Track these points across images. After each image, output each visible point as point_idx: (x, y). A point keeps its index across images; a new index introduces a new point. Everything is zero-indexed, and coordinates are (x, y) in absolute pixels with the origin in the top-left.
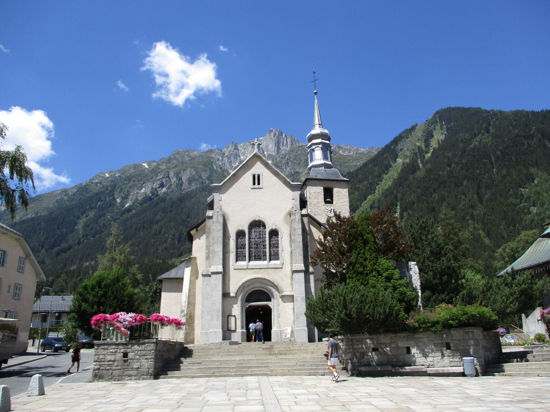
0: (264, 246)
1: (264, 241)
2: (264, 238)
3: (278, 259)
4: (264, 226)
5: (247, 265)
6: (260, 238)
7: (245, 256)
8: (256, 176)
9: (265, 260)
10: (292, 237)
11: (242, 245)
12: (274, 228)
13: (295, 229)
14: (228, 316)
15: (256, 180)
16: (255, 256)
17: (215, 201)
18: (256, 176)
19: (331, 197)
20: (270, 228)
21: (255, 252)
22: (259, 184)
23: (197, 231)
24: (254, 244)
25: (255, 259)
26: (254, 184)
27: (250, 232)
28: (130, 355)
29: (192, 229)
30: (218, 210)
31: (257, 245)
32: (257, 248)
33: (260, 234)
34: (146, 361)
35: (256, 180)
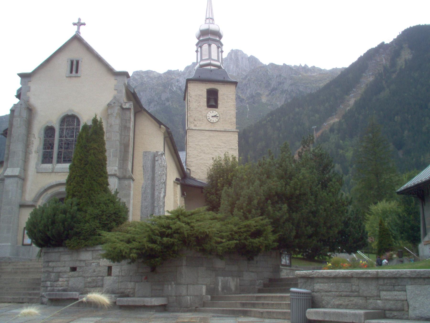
5: (53, 168)
6: (72, 136)
8: (75, 63)
11: (50, 144)
16: (64, 158)
18: (75, 63)
21: (65, 153)
22: (77, 72)
24: (65, 144)
25: (64, 161)
26: (71, 72)
27: (62, 130)
31: (68, 144)
32: (67, 148)
33: (73, 132)
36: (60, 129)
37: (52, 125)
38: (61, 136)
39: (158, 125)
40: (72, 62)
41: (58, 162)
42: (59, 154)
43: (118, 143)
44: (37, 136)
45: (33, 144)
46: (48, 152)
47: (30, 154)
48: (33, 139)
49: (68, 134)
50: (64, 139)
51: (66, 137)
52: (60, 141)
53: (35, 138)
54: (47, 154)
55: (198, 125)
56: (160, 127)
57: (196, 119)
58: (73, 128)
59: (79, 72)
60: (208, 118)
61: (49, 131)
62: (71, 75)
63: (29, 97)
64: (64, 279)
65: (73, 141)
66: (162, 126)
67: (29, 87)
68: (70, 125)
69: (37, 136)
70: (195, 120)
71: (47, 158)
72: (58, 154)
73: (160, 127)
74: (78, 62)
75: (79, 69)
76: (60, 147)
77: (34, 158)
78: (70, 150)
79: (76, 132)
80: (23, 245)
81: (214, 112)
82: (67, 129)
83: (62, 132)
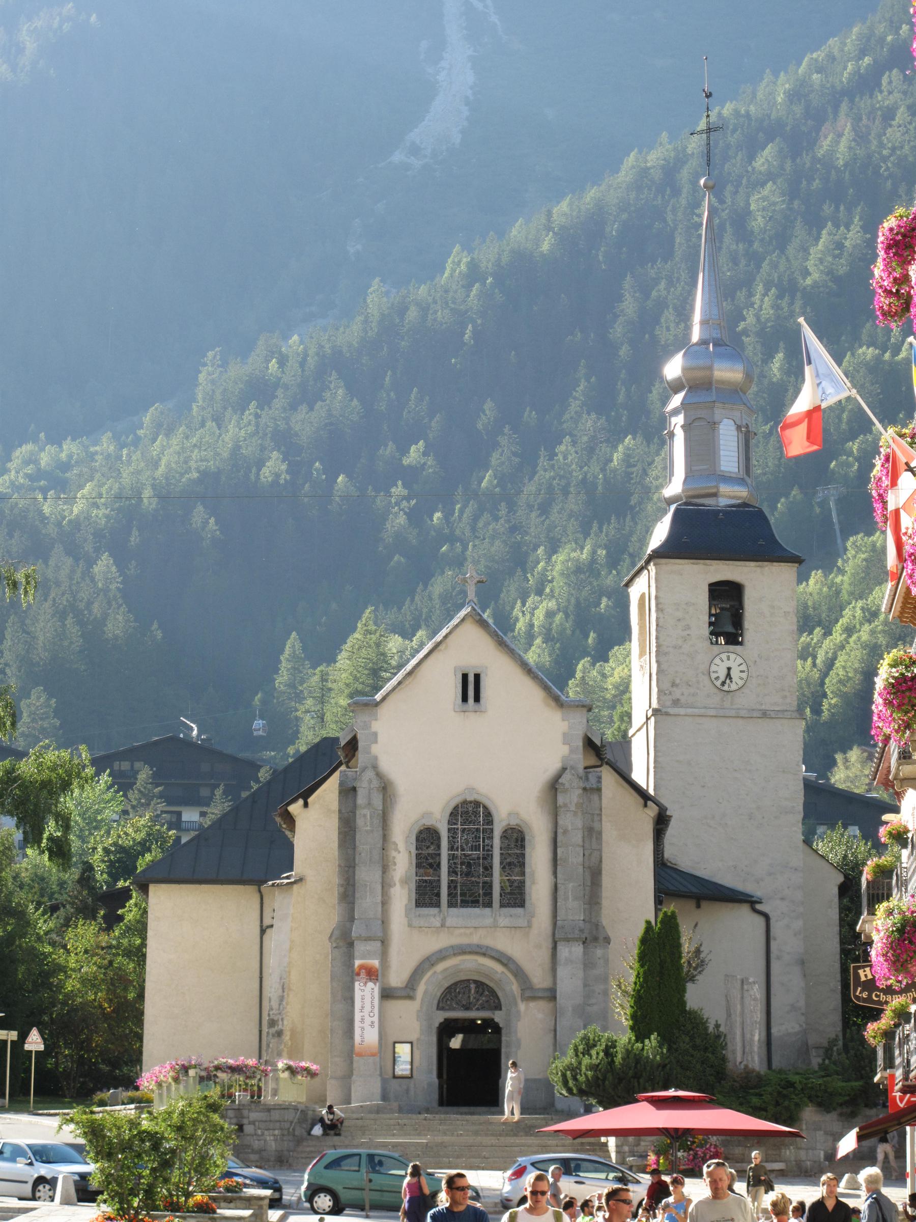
0: (486, 868)
1: (488, 856)
2: (489, 850)
3: (522, 904)
4: (488, 815)
6: (477, 848)
7: (438, 895)
8: (471, 679)
9: (489, 905)
10: (559, 851)
12: (513, 822)
13: (565, 832)
14: (395, 1043)
15: (471, 688)
16: (462, 895)
17: (361, 744)
18: (471, 679)
19: (737, 619)
20: (504, 824)
21: (463, 885)
22: (477, 699)
23: (306, 805)
24: (462, 864)
25: (462, 901)
26: (465, 699)
27: (452, 832)
28: (248, 1129)
29: (294, 800)
30: (370, 774)
32: (468, 874)
33: (477, 838)
34: (272, 1138)
35: (471, 688)
36: (449, 830)
37: (434, 823)
38: (451, 848)
39: (641, 801)
40: (465, 677)
41: (451, 905)
42: (452, 885)
43: (581, 869)
44: (401, 846)
45: (395, 864)
46: (426, 881)
47: (390, 886)
48: (394, 853)
49: (467, 843)
50: (459, 853)
51: (463, 850)
52: (452, 858)
53: (399, 852)
54: (425, 887)
55: (683, 700)
56: (646, 805)
57: (678, 681)
58: (478, 830)
59: (482, 701)
60: (713, 676)
61: (426, 837)
62: (465, 707)
63: (376, 758)
64: (647, 1144)
65: (479, 858)
66: (649, 803)
67: (375, 734)
68: (470, 822)
69: (401, 846)
70: (674, 684)
71: (426, 895)
72: (449, 887)
73: (646, 805)
74: (477, 677)
75: (482, 695)
76: (452, 871)
77: (401, 897)
78: (473, 879)
79: (484, 839)
80: (395, 1077)
81: (732, 656)
82: (463, 830)
83: (454, 838)
